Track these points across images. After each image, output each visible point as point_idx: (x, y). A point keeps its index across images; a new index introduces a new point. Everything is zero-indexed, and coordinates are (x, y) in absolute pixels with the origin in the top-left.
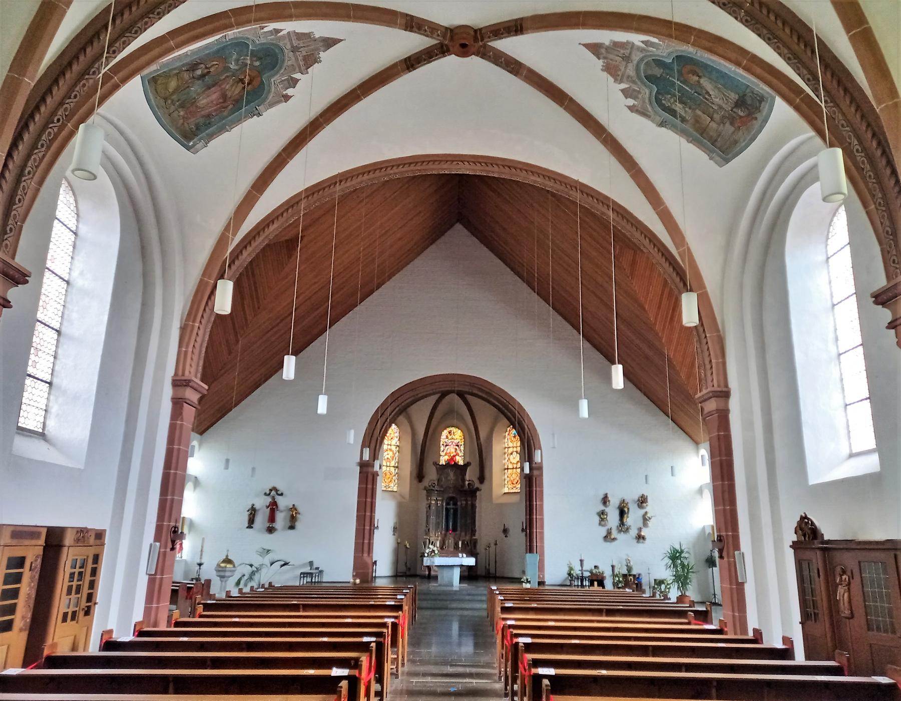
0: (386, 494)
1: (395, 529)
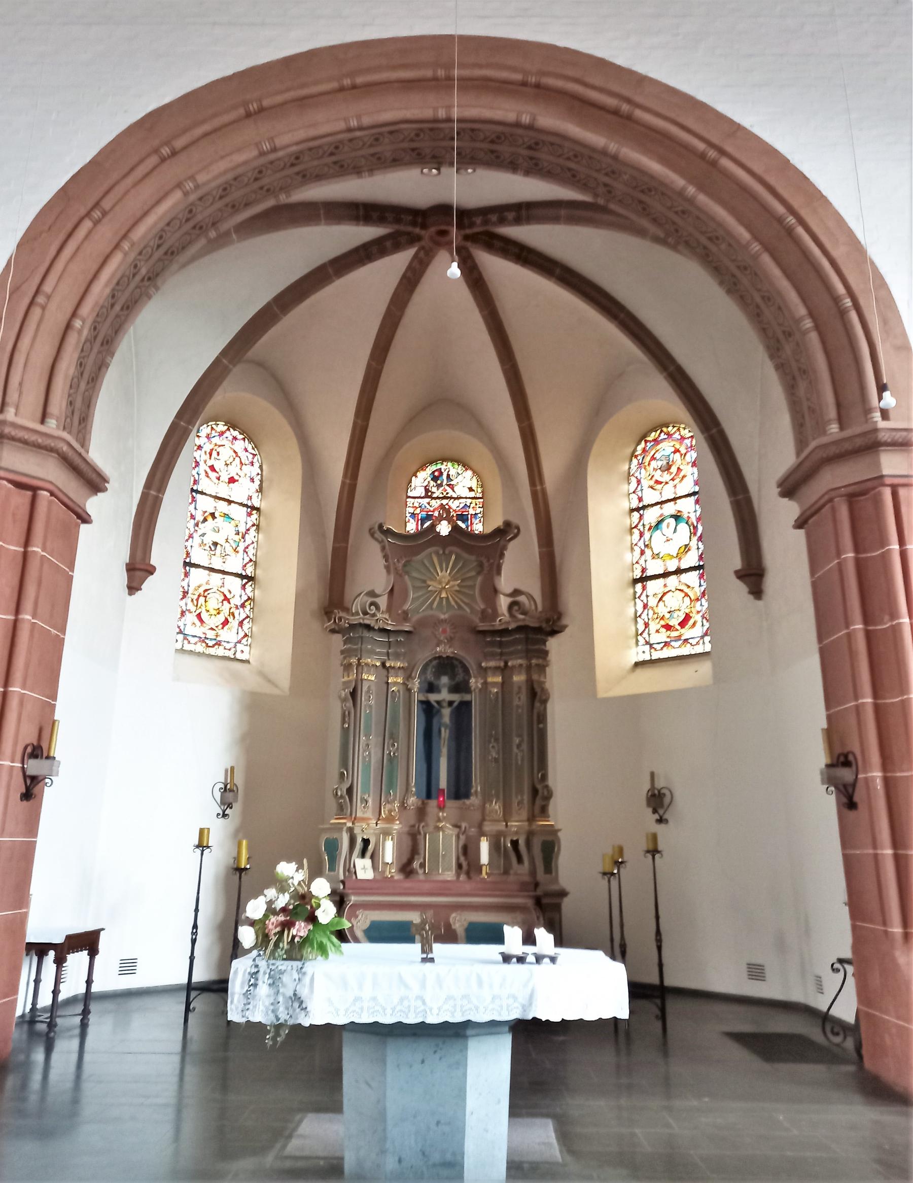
0: (187, 659)
1: (228, 795)
